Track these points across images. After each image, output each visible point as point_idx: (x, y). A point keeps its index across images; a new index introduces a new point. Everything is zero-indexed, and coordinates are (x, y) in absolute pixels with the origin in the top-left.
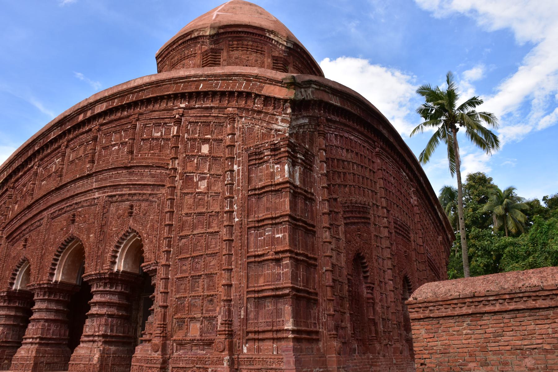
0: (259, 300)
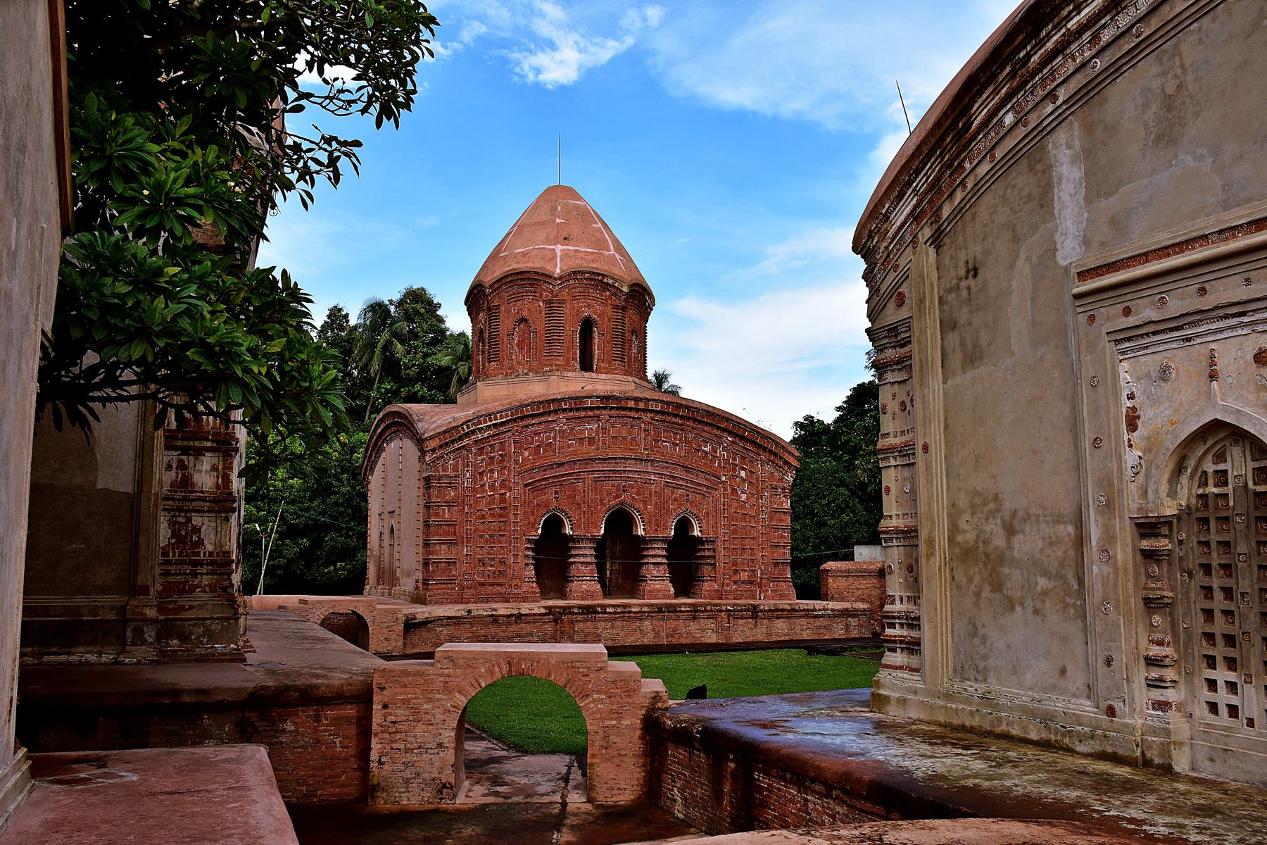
0: (776, 564)
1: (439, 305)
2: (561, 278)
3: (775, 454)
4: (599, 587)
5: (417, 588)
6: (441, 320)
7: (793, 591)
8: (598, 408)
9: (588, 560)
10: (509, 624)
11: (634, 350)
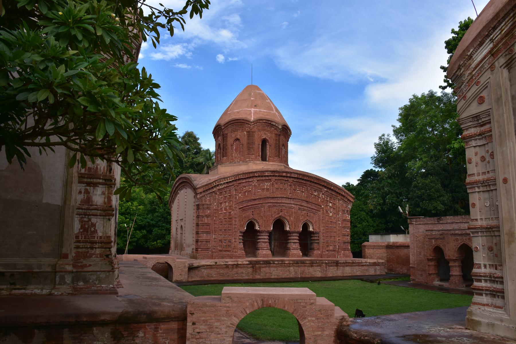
1: (198, 139)
2: (253, 122)
3: (344, 196)
4: (270, 252)
5: (193, 252)
6: (199, 144)
7: (351, 255)
8: (270, 176)
9: (266, 241)
10: (233, 268)
11: (283, 153)
